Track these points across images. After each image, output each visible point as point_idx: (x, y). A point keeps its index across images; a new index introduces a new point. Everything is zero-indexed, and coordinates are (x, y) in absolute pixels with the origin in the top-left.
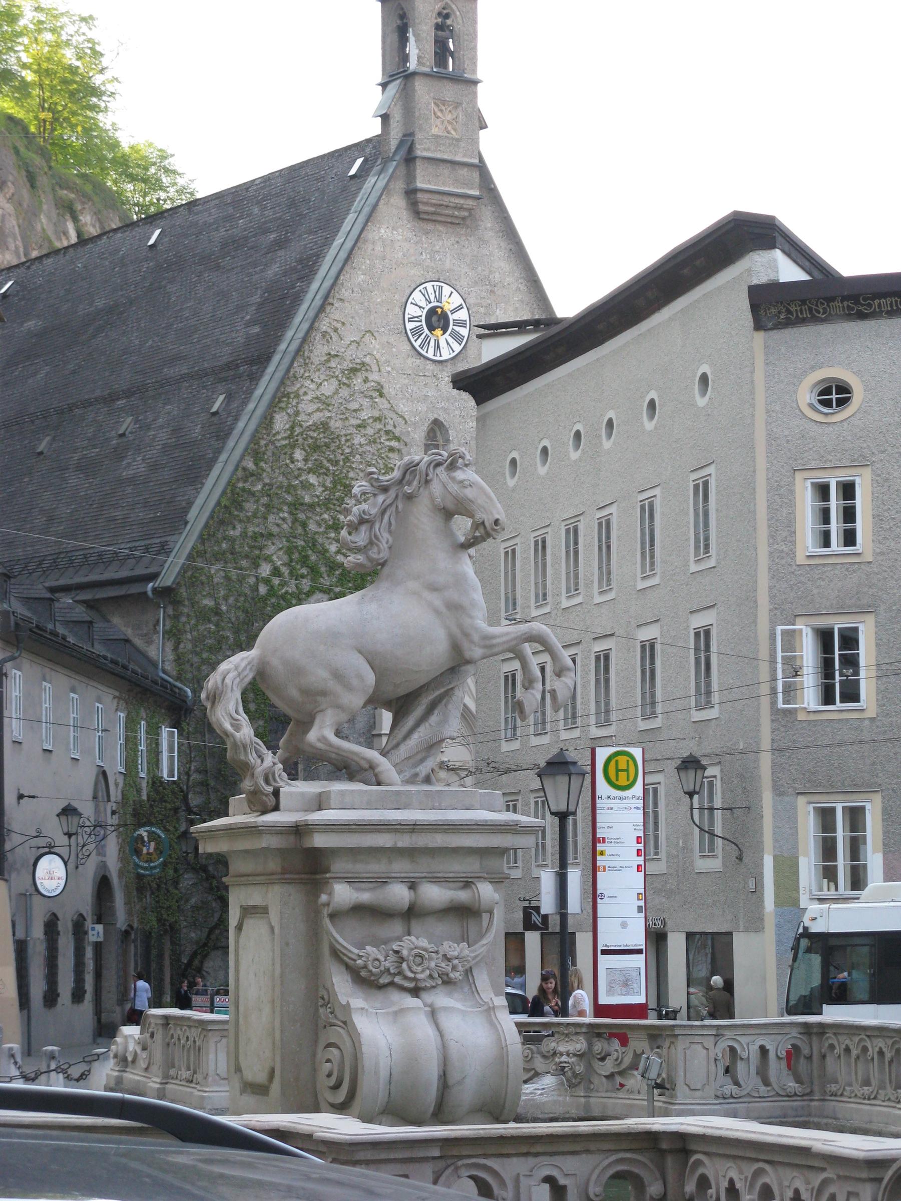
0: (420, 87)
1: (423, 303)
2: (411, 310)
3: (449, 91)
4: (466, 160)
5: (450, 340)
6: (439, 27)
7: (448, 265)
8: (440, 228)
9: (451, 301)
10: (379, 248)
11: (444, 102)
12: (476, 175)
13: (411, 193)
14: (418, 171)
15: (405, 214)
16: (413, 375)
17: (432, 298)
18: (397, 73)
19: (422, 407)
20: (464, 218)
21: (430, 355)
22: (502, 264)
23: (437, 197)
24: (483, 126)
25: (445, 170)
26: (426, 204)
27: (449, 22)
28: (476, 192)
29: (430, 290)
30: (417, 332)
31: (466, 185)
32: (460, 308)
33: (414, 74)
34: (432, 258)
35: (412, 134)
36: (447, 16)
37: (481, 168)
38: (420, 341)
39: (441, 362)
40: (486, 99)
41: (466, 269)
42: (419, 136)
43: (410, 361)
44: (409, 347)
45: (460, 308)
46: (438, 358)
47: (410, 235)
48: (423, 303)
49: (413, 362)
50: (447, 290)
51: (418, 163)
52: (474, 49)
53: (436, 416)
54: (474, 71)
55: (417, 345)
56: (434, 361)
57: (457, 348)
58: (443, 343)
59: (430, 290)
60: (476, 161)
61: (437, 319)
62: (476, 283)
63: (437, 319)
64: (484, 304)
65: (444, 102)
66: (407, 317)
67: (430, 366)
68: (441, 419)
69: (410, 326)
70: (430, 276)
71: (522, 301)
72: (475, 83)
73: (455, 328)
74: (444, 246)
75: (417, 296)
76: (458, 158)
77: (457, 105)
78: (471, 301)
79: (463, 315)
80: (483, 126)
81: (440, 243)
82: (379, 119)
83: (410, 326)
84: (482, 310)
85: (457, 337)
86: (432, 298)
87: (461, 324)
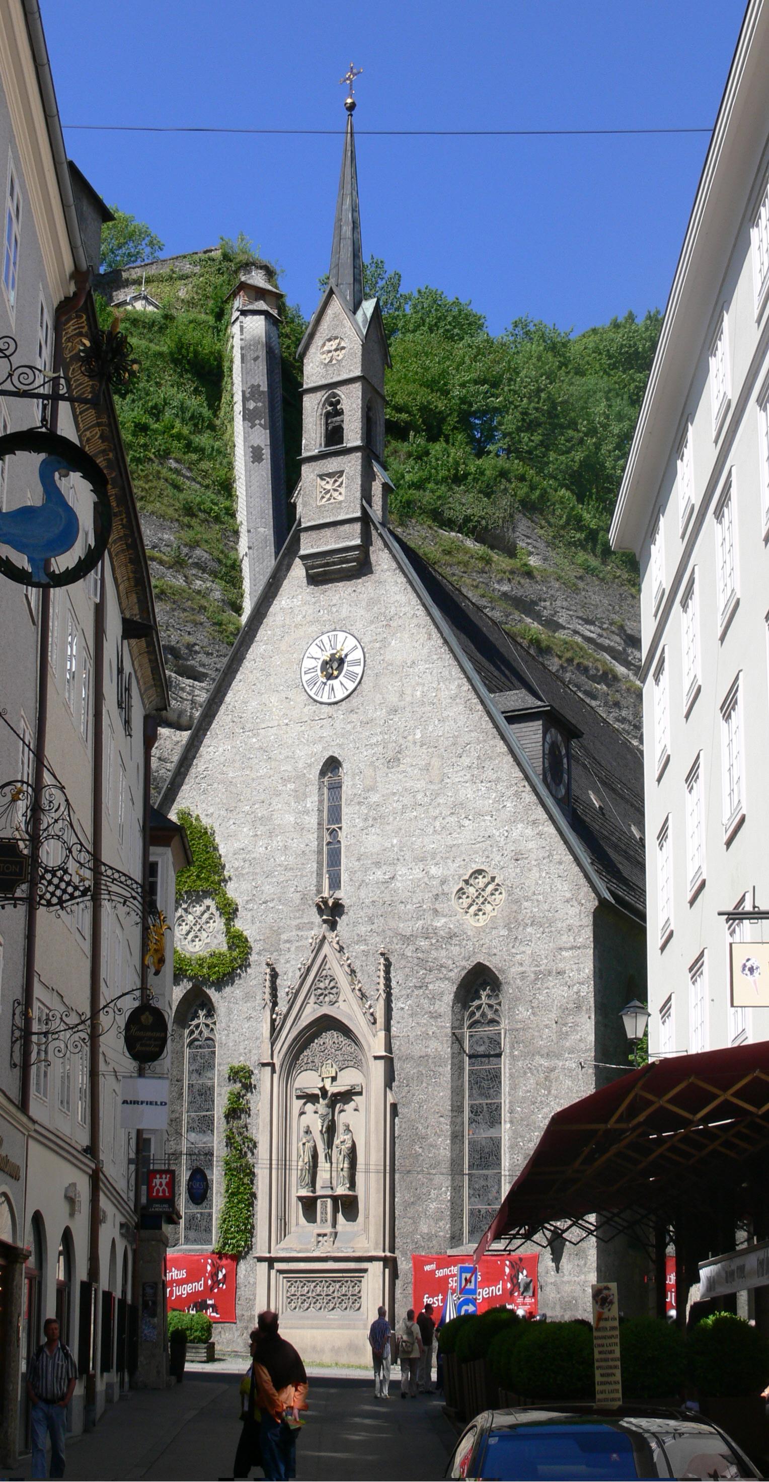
7: (344, 612)
9: (346, 644)
11: (330, 475)
16: (309, 722)
17: (328, 647)
19: (318, 748)
21: (325, 700)
25: (328, 532)
32: (355, 648)
34: (330, 612)
38: (315, 688)
39: (336, 703)
41: (362, 612)
44: (306, 697)
45: (355, 648)
46: (333, 700)
47: (308, 598)
50: (341, 636)
53: (331, 754)
55: (312, 694)
56: (330, 704)
57: (351, 686)
61: (334, 666)
62: (372, 622)
64: (380, 638)
65: (330, 475)
66: (303, 670)
68: (336, 755)
69: (305, 678)
70: (328, 628)
71: (418, 626)
73: (350, 669)
75: (314, 650)
77: (341, 473)
78: (366, 640)
81: (337, 596)
83: (305, 678)
84: (378, 645)
85: (351, 676)
86: (328, 647)
87: (356, 663)
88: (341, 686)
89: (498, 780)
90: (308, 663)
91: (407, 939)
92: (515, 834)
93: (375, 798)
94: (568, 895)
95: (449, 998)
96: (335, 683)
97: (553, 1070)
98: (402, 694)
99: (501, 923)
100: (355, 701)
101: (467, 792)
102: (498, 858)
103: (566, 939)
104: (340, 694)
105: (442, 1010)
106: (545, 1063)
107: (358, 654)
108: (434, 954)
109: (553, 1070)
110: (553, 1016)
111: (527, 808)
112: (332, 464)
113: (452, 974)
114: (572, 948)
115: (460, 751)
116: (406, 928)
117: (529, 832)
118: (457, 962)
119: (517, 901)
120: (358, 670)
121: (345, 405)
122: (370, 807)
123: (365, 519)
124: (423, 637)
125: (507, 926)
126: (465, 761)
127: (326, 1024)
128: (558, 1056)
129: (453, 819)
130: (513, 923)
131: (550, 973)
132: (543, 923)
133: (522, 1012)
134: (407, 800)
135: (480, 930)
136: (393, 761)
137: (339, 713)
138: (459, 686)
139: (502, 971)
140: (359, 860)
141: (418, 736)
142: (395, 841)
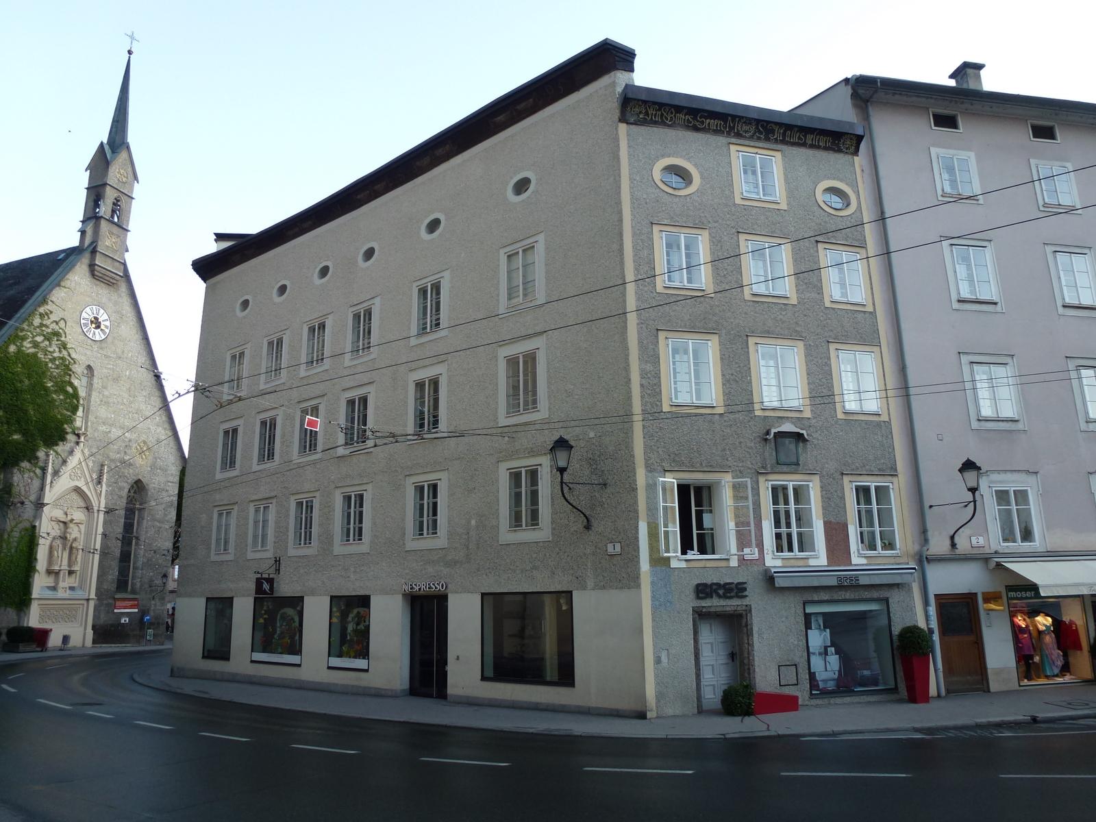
0: (103, 223)
1: (90, 314)
2: (84, 315)
3: (115, 229)
4: (118, 259)
6: (114, 204)
8: (102, 284)
9: (103, 317)
11: (113, 234)
12: (122, 267)
13: (92, 266)
14: (97, 257)
15: (88, 274)
17: (95, 313)
18: (92, 217)
20: (113, 284)
21: (90, 336)
22: (128, 308)
23: (104, 270)
24: (127, 251)
25: (109, 261)
26: (98, 271)
27: (119, 203)
28: (122, 275)
29: (95, 309)
30: (86, 325)
31: (116, 269)
33: (102, 217)
35: (97, 241)
36: (118, 201)
37: (125, 264)
40: (131, 239)
42: (100, 243)
43: (80, 336)
44: (81, 330)
46: (94, 339)
47: (89, 284)
48: (90, 314)
49: (82, 337)
50: (102, 311)
51: (98, 253)
52: (129, 217)
54: (127, 226)
57: (103, 337)
58: (97, 333)
59: (95, 309)
60: (123, 262)
62: (115, 312)
63: (96, 323)
65: (113, 234)
67: (89, 341)
71: (133, 325)
72: (128, 231)
74: (103, 292)
76: (115, 258)
79: (108, 323)
80: (127, 251)
82: (80, 233)
83: (83, 321)
86: (95, 313)
87: (106, 327)
88: (99, 335)
89: (155, 406)
91: (112, 461)
92: (158, 431)
93: (106, 393)
94: (173, 462)
95: (126, 490)
97: (161, 528)
98: (123, 352)
99: (149, 465)
100: (104, 345)
101: (143, 407)
102: (151, 438)
103: (171, 479)
104: (98, 338)
105: (123, 495)
106: (158, 524)
108: (123, 470)
109: (161, 528)
110: (163, 506)
113: (129, 481)
114: (171, 482)
115: (142, 388)
116: (113, 455)
117: (163, 431)
118: (131, 475)
119: (156, 458)
122: (103, 395)
124: (135, 331)
125: (151, 467)
127: (77, 490)
128: (163, 522)
129: (136, 415)
130: (153, 466)
131: (163, 490)
132: (164, 470)
133: (153, 503)
135: (141, 466)
136: (116, 380)
137: (95, 347)
138: (145, 360)
139: (147, 485)
140: (96, 418)
141: (127, 373)
142: (113, 416)
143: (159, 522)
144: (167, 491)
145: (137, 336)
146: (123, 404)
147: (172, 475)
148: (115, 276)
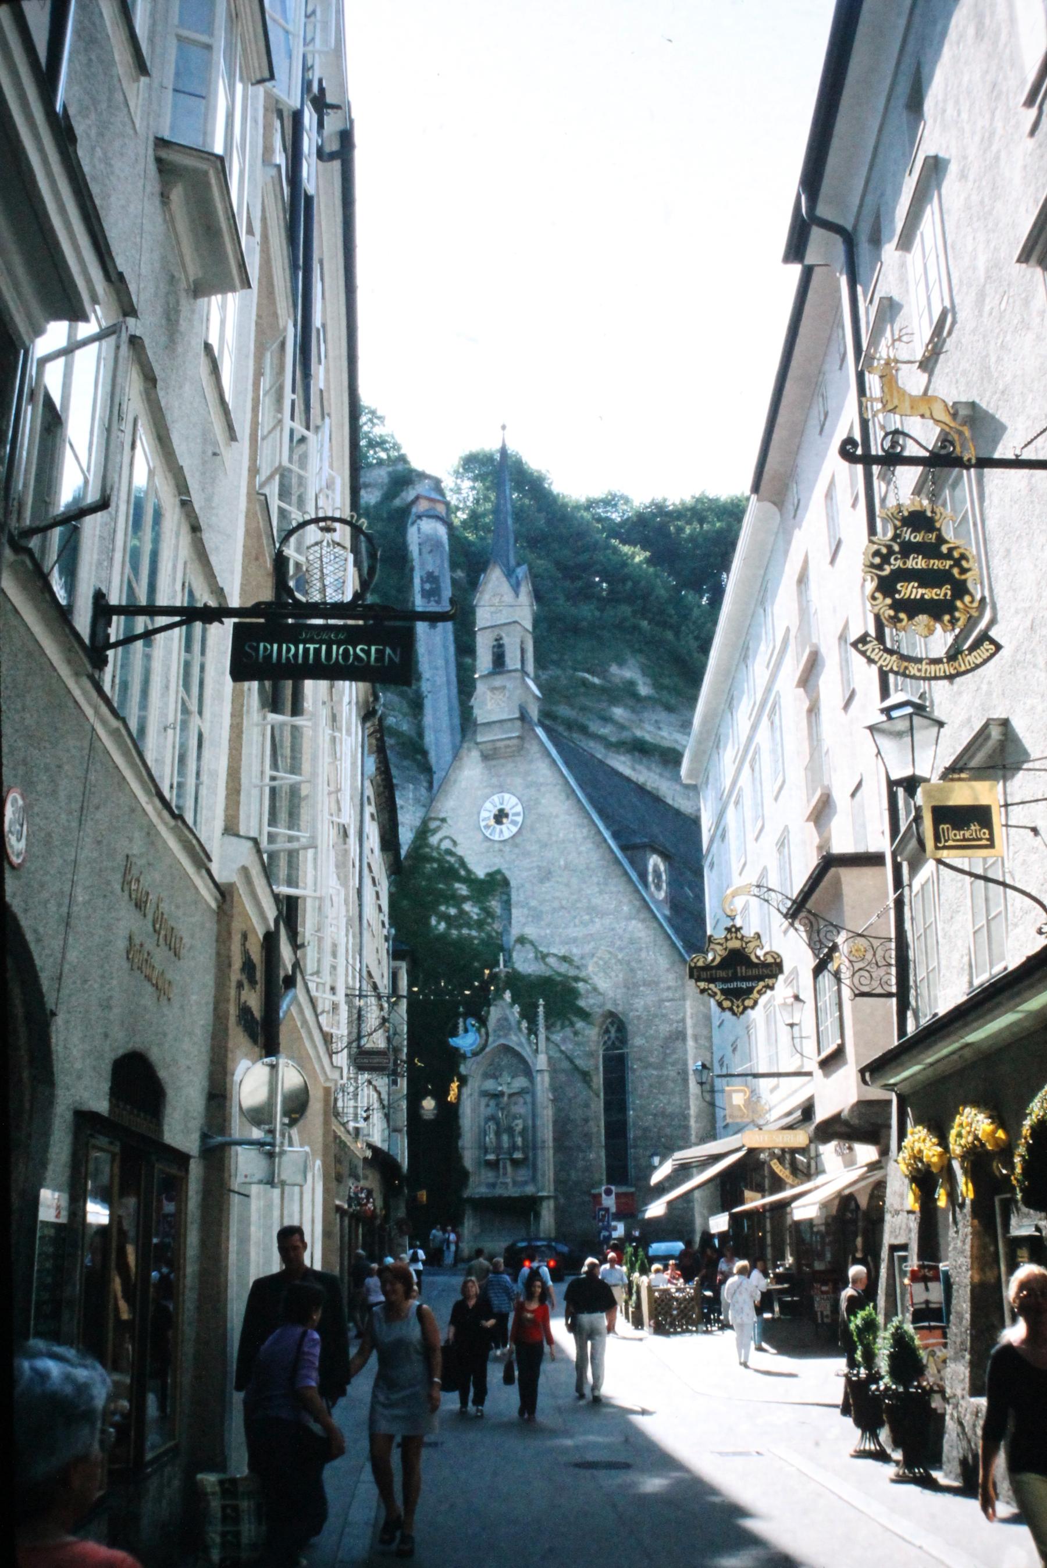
5: (511, 827)
9: (511, 803)
10: (463, 784)
57: (515, 829)
61: (500, 816)
67: (497, 846)
69: (482, 824)
75: (488, 805)
83: (482, 824)
85: (514, 823)
88: (508, 830)
90: (484, 814)
92: (630, 928)
96: (503, 827)
100: (518, 840)
101: (597, 901)
104: (507, 835)
106: (655, 1073)
107: (519, 809)
111: (638, 911)
112: (498, 681)
120: (520, 819)
121: (506, 641)
123: (523, 717)
126: (595, 879)
133: (638, 1041)
134: (556, 904)
141: (562, 863)
143: (656, 1069)
144: (663, 1016)
145: (567, 803)
146: (562, 907)
147: (669, 988)
148: (508, 742)
